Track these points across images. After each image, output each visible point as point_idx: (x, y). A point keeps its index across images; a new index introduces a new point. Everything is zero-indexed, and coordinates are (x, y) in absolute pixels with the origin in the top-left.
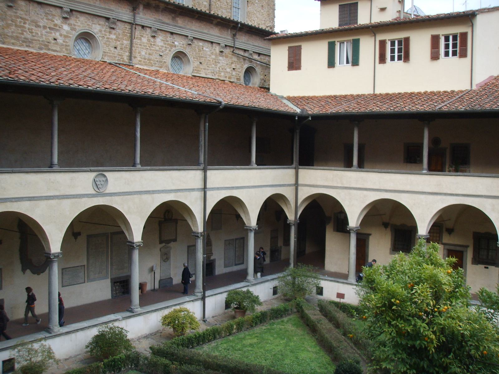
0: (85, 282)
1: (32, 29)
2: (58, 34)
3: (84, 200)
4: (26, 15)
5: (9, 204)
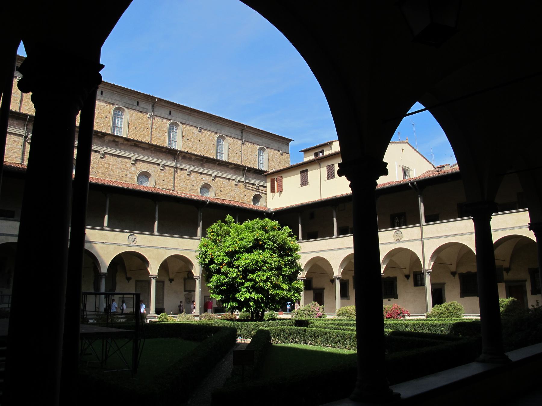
2: (128, 172)
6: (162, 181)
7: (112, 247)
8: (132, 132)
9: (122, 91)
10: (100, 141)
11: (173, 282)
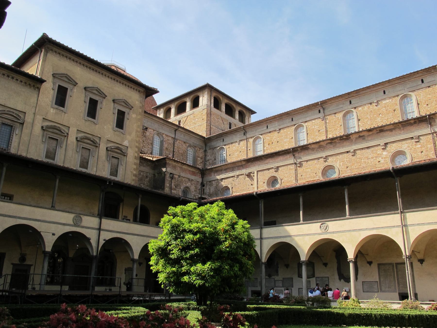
0: (378, 292)
1: (366, 161)
2: (380, 158)
6: (420, 154)
7: (307, 238)
8: (424, 110)
9: (401, 80)
10: (348, 142)
11: (424, 262)
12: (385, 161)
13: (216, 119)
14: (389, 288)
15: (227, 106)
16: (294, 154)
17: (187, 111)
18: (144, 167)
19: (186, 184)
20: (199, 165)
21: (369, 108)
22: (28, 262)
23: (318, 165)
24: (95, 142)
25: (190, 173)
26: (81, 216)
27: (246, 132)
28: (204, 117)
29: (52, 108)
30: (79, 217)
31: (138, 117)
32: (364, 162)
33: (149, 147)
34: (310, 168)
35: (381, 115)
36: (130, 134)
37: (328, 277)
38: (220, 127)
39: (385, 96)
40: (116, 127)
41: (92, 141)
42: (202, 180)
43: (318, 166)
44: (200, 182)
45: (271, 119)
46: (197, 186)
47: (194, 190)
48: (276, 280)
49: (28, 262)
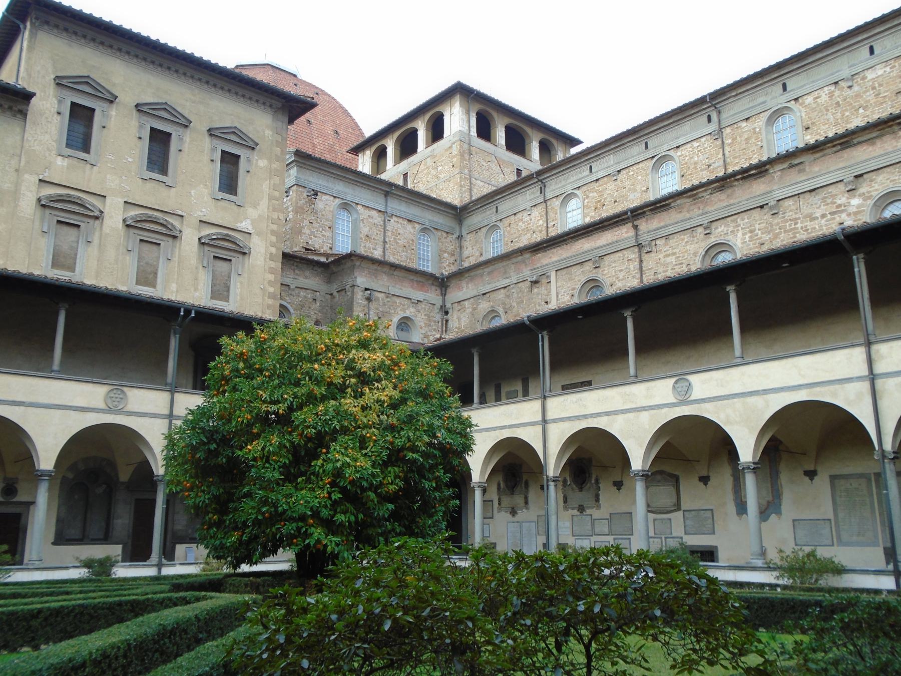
0: (833, 545)
1: (806, 226)
2: (844, 216)
3: (665, 410)
4: (796, 213)
5: (590, 420)
7: (645, 415)
12: (855, 221)
13: (482, 163)
14: (859, 535)
15: (509, 130)
16: (636, 223)
17: (419, 150)
18: (306, 278)
19: (404, 310)
20: (447, 268)
21: (831, 95)
22: (21, 497)
23: (693, 246)
24: (170, 227)
25: (412, 287)
26: (125, 389)
27: (545, 186)
28: (455, 160)
29: (60, 155)
30: (119, 392)
31: (274, 166)
32: (802, 228)
33: (324, 236)
34: (674, 254)
35: (861, 111)
36: (255, 206)
37: (712, 510)
38: (493, 183)
39: (874, 60)
40: (220, 190)
41: (162, 225)
42: (444, 301)
43: (691, 248)
44: (438, 305)
45: (600, 149)
46: (432, 314)
47: (425, 323)
48: (594, 519)
49: (21, 497)
